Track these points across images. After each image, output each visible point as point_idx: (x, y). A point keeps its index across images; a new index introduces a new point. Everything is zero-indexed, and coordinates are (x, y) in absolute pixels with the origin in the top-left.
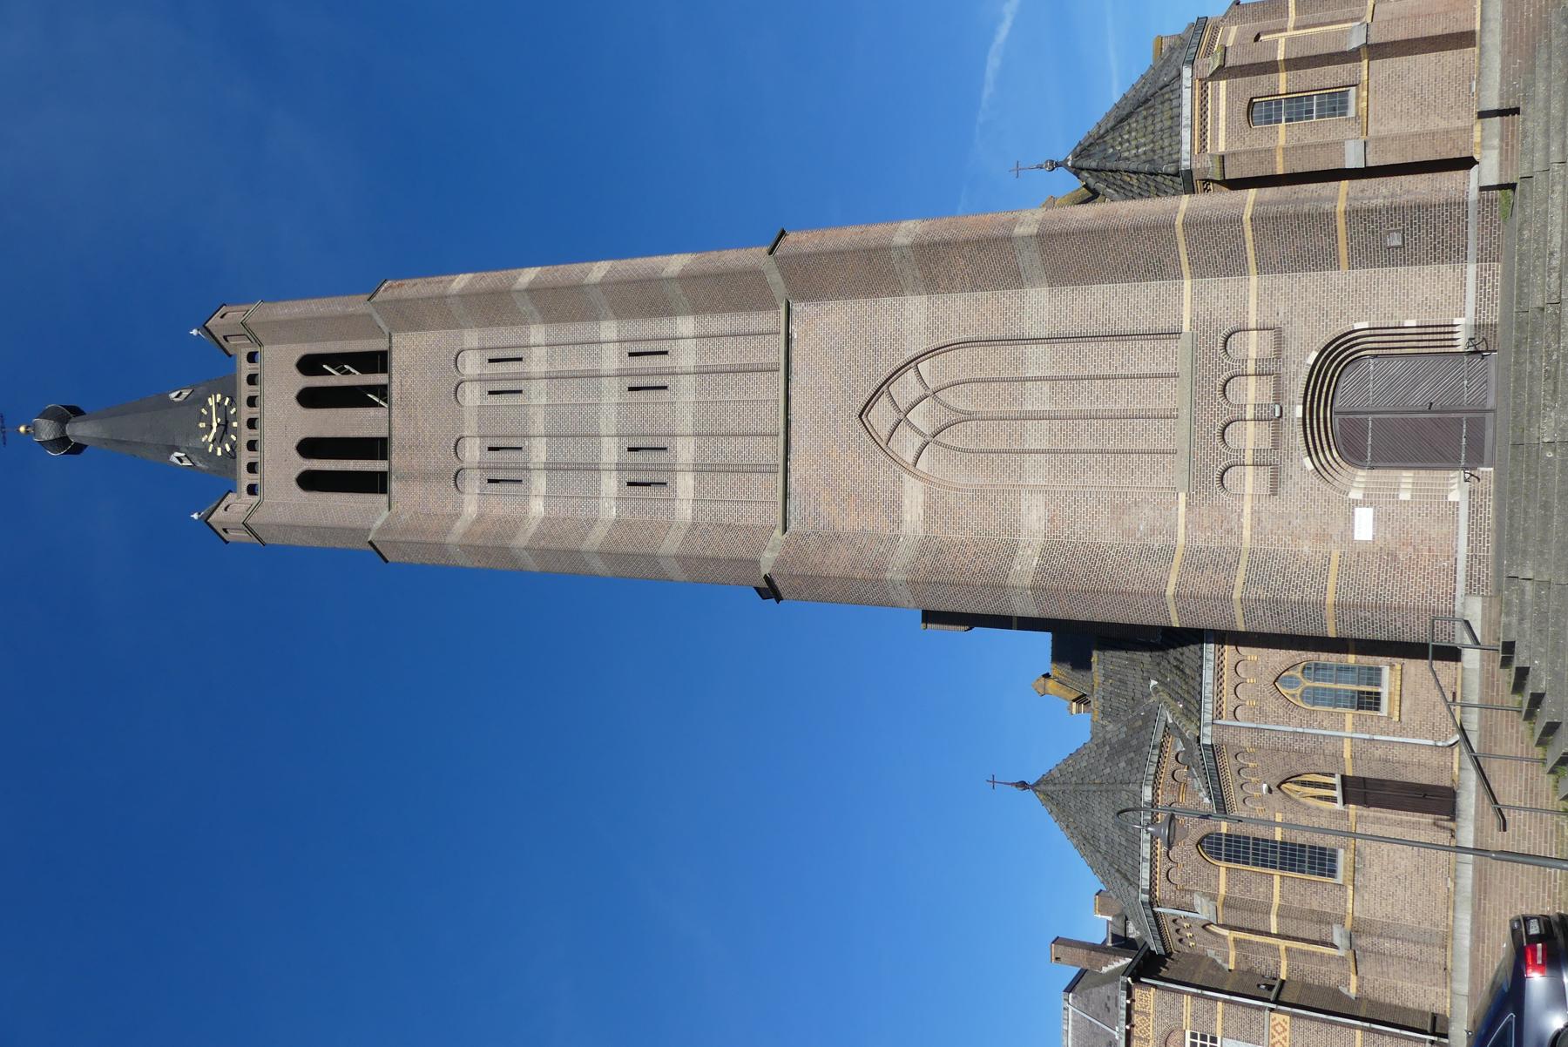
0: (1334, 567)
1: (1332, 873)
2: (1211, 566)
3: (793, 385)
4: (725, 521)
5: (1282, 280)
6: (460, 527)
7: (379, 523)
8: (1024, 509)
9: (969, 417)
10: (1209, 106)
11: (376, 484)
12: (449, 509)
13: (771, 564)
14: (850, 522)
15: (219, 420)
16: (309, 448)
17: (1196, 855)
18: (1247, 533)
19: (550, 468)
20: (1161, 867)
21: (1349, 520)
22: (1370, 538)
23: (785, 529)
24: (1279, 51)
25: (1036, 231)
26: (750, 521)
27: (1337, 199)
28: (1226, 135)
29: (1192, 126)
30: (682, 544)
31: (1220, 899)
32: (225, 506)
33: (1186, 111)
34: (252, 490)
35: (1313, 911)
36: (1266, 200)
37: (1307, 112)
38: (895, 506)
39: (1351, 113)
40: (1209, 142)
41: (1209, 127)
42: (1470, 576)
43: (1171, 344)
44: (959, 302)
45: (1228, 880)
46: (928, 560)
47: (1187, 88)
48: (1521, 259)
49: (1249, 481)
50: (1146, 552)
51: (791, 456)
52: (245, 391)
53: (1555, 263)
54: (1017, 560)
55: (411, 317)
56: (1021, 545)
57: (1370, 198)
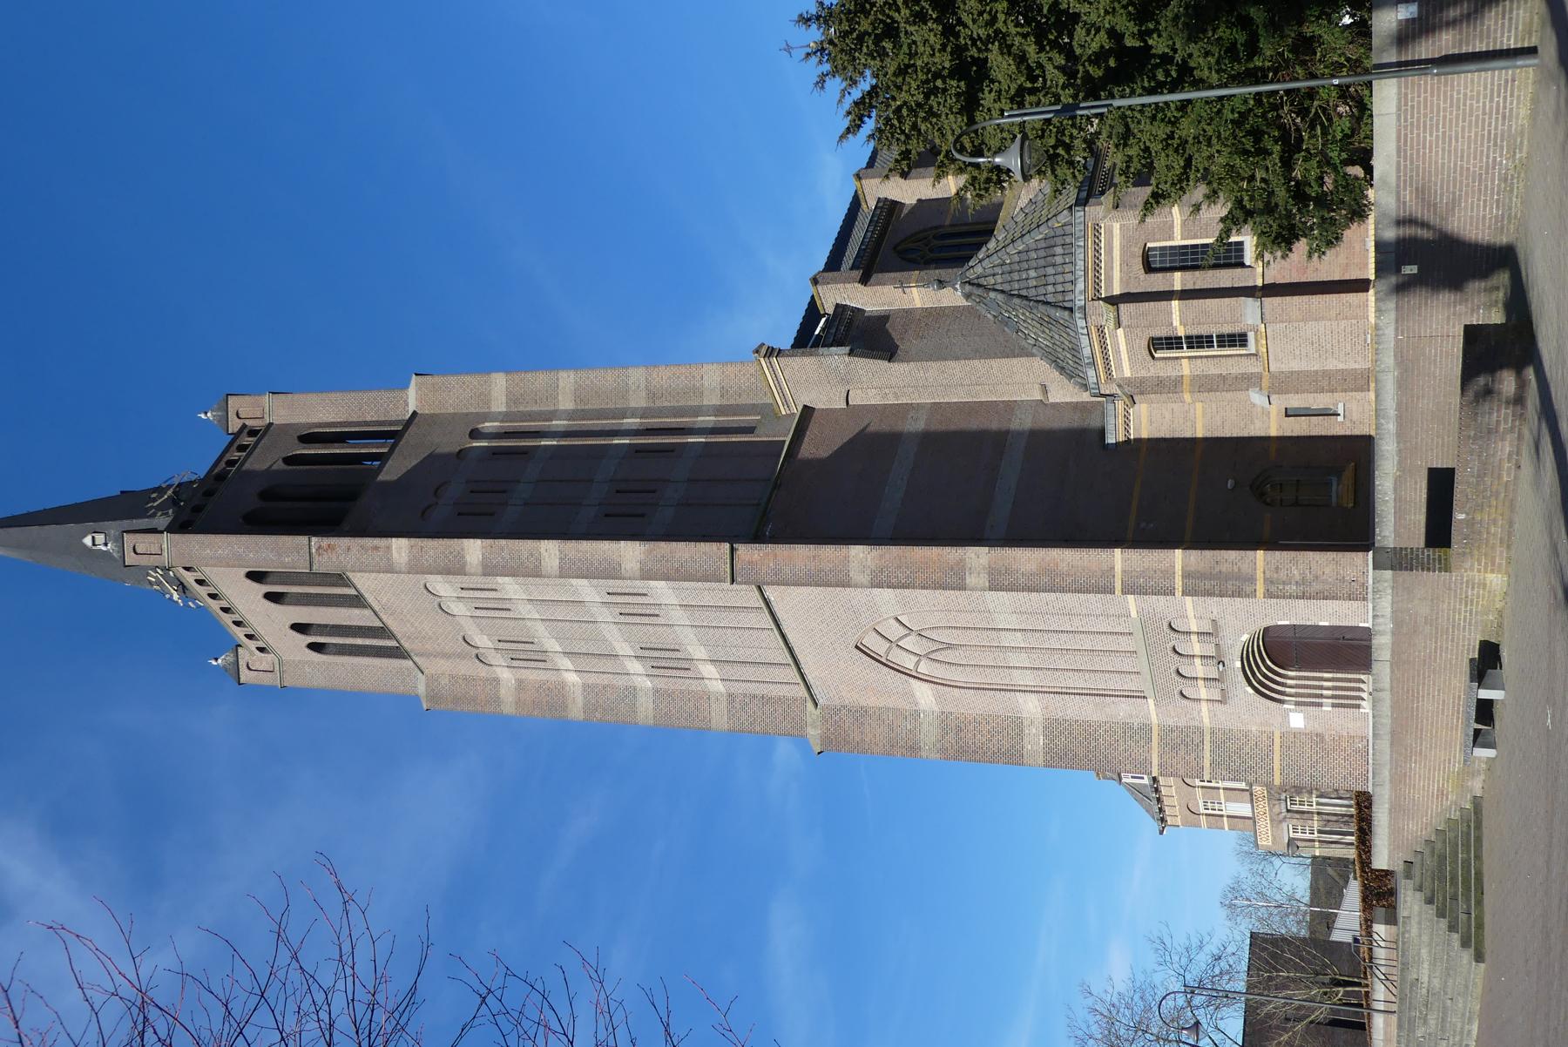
0: (1277, 747)
6: (507, 693)
10: (1108, 341)
11: (398, 653)
14: (871, 701)
23: (816, 705)
24: (1174, 316)
27: (1256, 580)
28: (1130, 365)
30: (729, 718)
36: (1193, 569)
38: (910, 695)
39: (1252, 348)
40: (1113, 369)
41: (1111, 358)
46: (951, 737)
47: (1082, 334)
54: (1026, 740)
56: (1025, 723)
57: (1284, 583)
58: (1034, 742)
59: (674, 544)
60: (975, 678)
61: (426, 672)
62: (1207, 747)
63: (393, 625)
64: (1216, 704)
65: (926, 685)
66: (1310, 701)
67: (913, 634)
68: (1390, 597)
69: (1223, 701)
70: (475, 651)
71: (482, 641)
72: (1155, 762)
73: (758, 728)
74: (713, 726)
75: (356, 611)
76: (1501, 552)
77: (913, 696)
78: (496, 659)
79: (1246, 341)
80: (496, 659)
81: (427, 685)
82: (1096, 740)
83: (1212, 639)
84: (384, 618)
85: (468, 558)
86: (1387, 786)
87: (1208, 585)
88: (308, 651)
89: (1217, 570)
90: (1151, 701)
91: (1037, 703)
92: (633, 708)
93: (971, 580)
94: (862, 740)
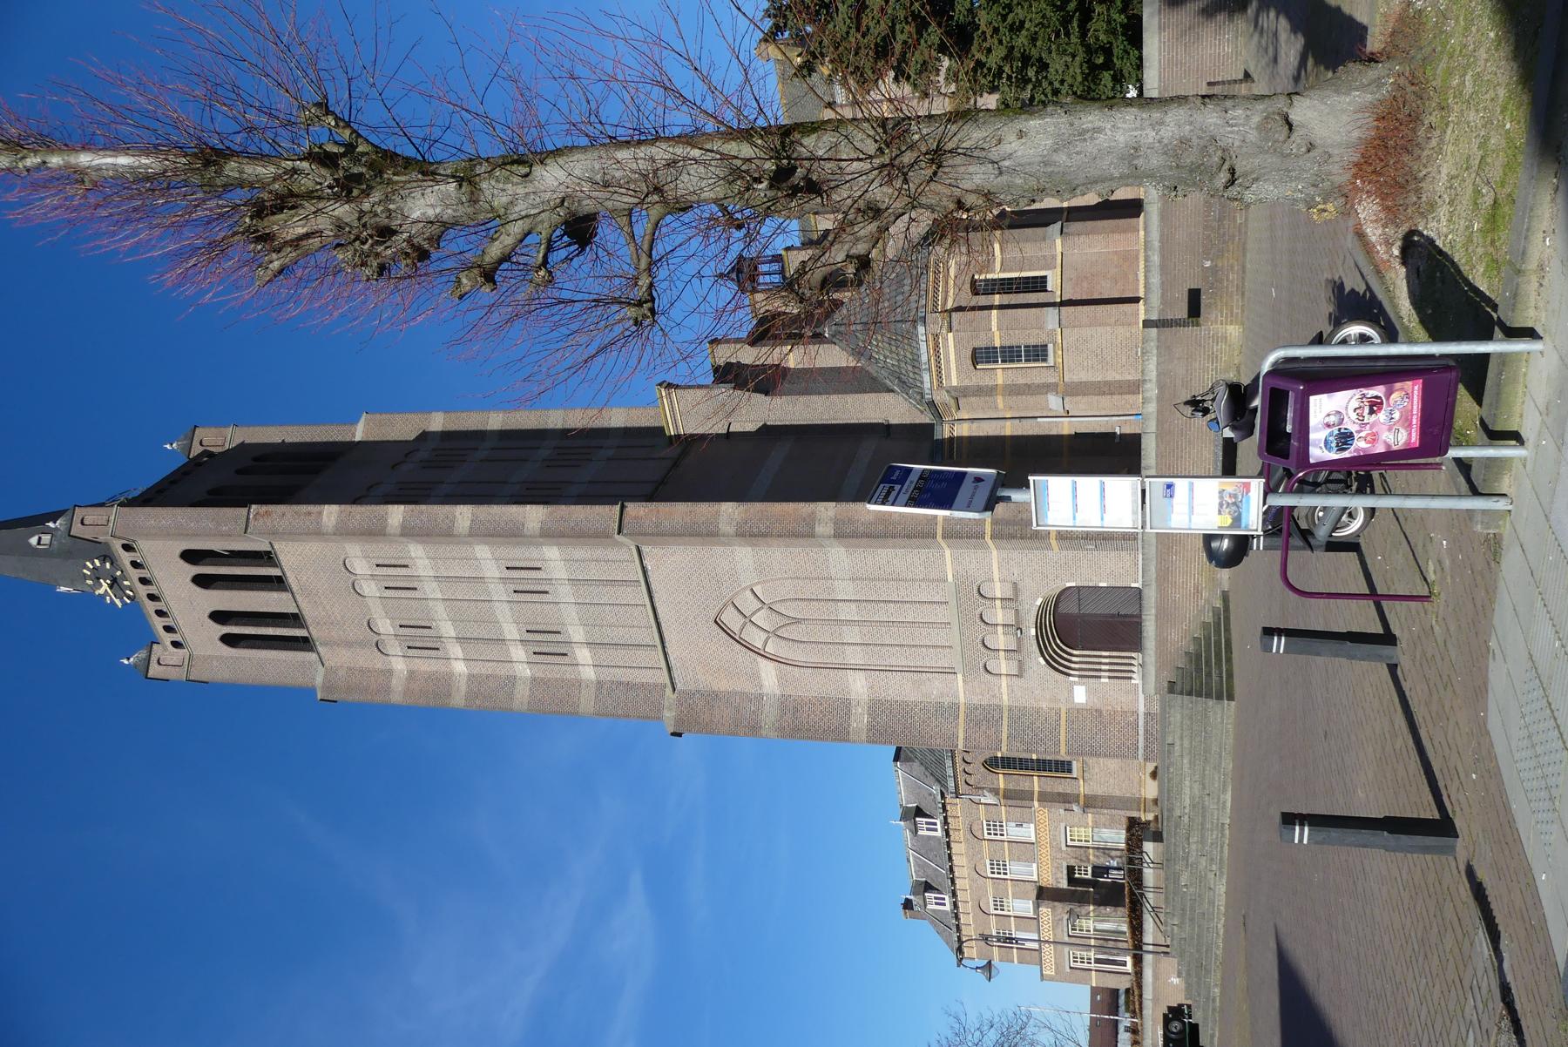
1: (1070, 771)
2: (984, 722)
3: (656, 600)
4: (624, 679)
5: (1015, 554)
6: (397, 684)
7: (319, 680)
8: (851, 680)
9: (798, 621)
10: (941, 351)
11: (305, 644)
12: (379, 666)
13: (672, 723)
14: (723, 685)
15: (109, 582)
16: (219, 617)
17: (983, 769)
18: (1005, 697)
19: (460, 639)
20: (961, 777)
21: (1071, 691)
22: (1084, 702)
25: (833, 532)
26: (643, 680)
29: (930, 370)
31: (1001, 792)
32: (79, 521)
33: (924, 358)
34: (176, 644)
35: (1059, 794)
37: (1017, 356)
38: (755, 676)
39: (1051, 361)
42: (1146, 731)
43: (941, 585)
44: (777, 553)
45: (1005, 780)
48: (1169, 782)
49: (1003, 665)
50: (939, 706)
51: (667, 644)
52: (125, 558)
53: (1187, 811)
54: (852, 718)
55: (292, 535)
56: (853, 703)
58: (860, 720)
59: (573, 507)
60: (814, 659)
61: (326, 664)
62: (1005, 722)
63: (308, 613)
64: (1014, 678)
65: (771, 664)
66: (1090, 674)
67: (765, 607)
68: (1155, 358)
69: (1019, 676)
70: (376, 638)
71: (385, 626)
72: (961, 736)
73: (620, 712)
74: (581, 711)
75: (275, 595)
76: (1238, 301)
77: (759, 677)
78: (394, 648)
79: (1047, 355)
80: (394, 648)
81: (325, 677)
82: (912, 717)
83: (1012, 604)
84: (303, 605)
85: (390, 521)
86: (1154, 587)
87: (1012, 530)
88: (220, 644)
89: (1019, 518)
90: (960, 676)
91: (864, 682)
92: (511, 696)
93: (819, 529)
94: (711, 721)
